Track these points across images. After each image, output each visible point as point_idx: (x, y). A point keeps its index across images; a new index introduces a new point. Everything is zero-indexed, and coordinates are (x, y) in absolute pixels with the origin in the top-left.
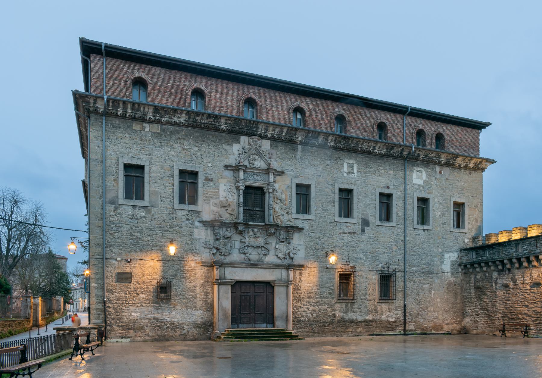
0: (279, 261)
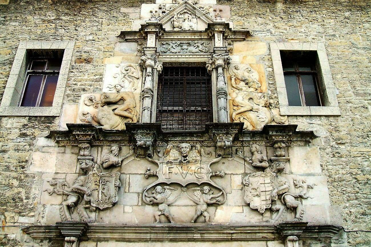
0: (255, 219)
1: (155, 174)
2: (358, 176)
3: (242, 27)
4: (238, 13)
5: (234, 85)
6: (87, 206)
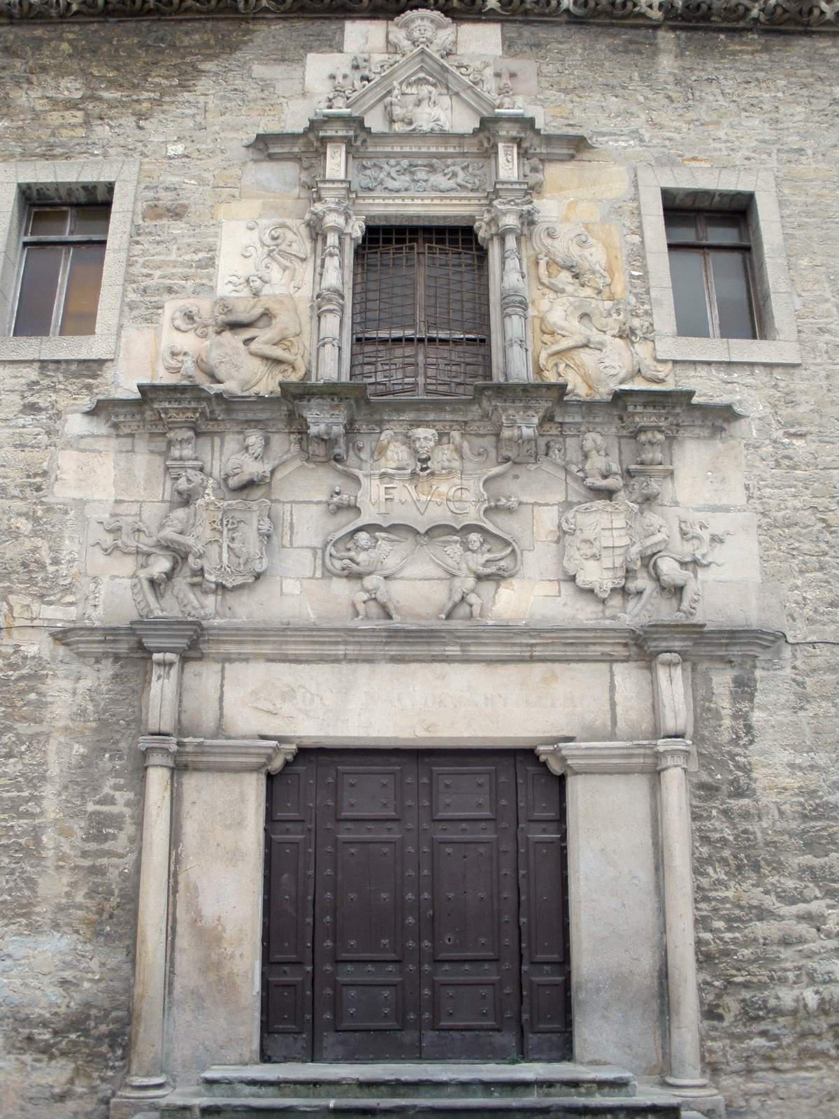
1: (352, 502)
2: (829, 516)
3: (566, 122)
4: (558, 83)
5: (545, 280)
6: (196, 580)
